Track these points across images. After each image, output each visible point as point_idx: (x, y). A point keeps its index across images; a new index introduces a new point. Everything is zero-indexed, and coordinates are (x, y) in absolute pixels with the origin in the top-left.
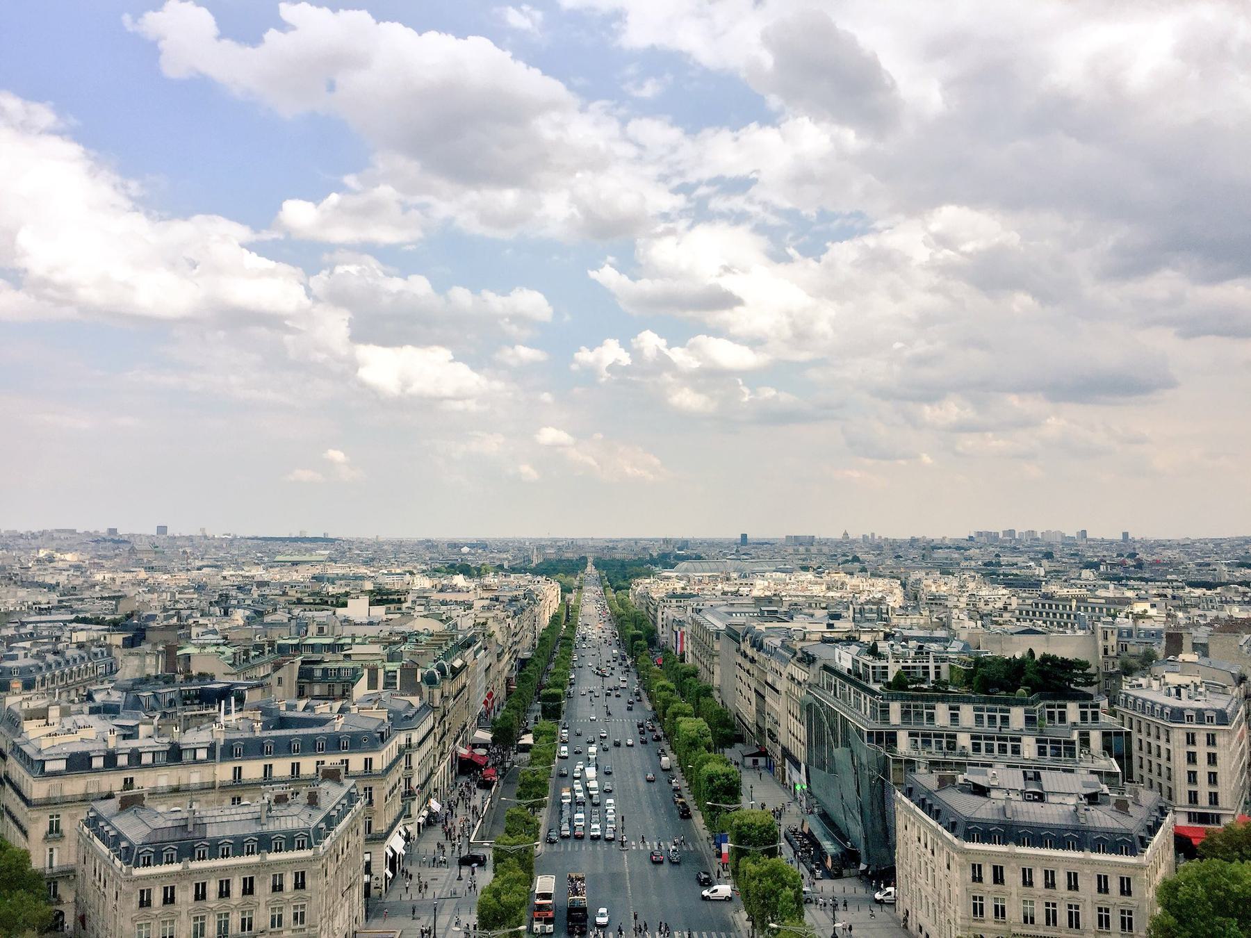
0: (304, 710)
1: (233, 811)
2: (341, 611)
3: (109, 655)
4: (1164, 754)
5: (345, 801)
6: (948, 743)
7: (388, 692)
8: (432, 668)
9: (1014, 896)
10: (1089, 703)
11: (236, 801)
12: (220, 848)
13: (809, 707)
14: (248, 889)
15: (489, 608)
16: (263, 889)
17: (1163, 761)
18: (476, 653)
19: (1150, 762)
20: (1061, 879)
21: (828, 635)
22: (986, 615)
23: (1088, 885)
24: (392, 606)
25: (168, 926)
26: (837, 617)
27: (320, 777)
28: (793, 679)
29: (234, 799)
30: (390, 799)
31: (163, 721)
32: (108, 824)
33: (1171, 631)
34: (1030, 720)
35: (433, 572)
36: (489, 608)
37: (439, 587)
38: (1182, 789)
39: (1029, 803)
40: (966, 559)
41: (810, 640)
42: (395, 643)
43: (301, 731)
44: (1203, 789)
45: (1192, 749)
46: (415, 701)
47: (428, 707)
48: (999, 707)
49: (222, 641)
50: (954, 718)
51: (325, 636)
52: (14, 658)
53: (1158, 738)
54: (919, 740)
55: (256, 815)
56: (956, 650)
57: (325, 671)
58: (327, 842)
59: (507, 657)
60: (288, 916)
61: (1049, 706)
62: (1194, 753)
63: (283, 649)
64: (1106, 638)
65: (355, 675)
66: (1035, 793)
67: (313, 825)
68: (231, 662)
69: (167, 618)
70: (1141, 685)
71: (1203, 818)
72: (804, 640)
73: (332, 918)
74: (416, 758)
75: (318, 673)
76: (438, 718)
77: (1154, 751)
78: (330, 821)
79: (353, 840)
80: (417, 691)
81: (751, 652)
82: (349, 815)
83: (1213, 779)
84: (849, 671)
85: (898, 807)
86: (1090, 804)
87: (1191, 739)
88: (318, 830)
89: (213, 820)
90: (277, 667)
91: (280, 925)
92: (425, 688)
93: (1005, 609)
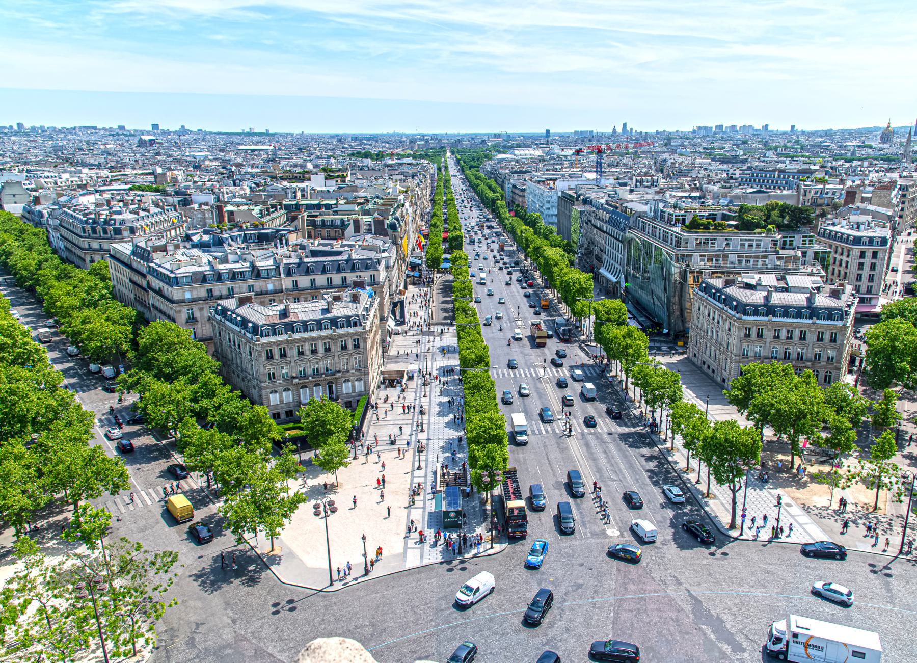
0: (319, 244)
4: (844, 264)
11: (297, 300)
16: (336, 348)
17: (842, 268)
42: (360, 204)
43: (330, 258)
45: (862, 261)
51: (306, 199)
53: (842, 254)
57: (323, 221)
58: (369, 323)
64: (805, 195)
75: (319, 223)
77: (837, 263)
78: (367, 310)
87: (862, 254)
92: (390, 231)
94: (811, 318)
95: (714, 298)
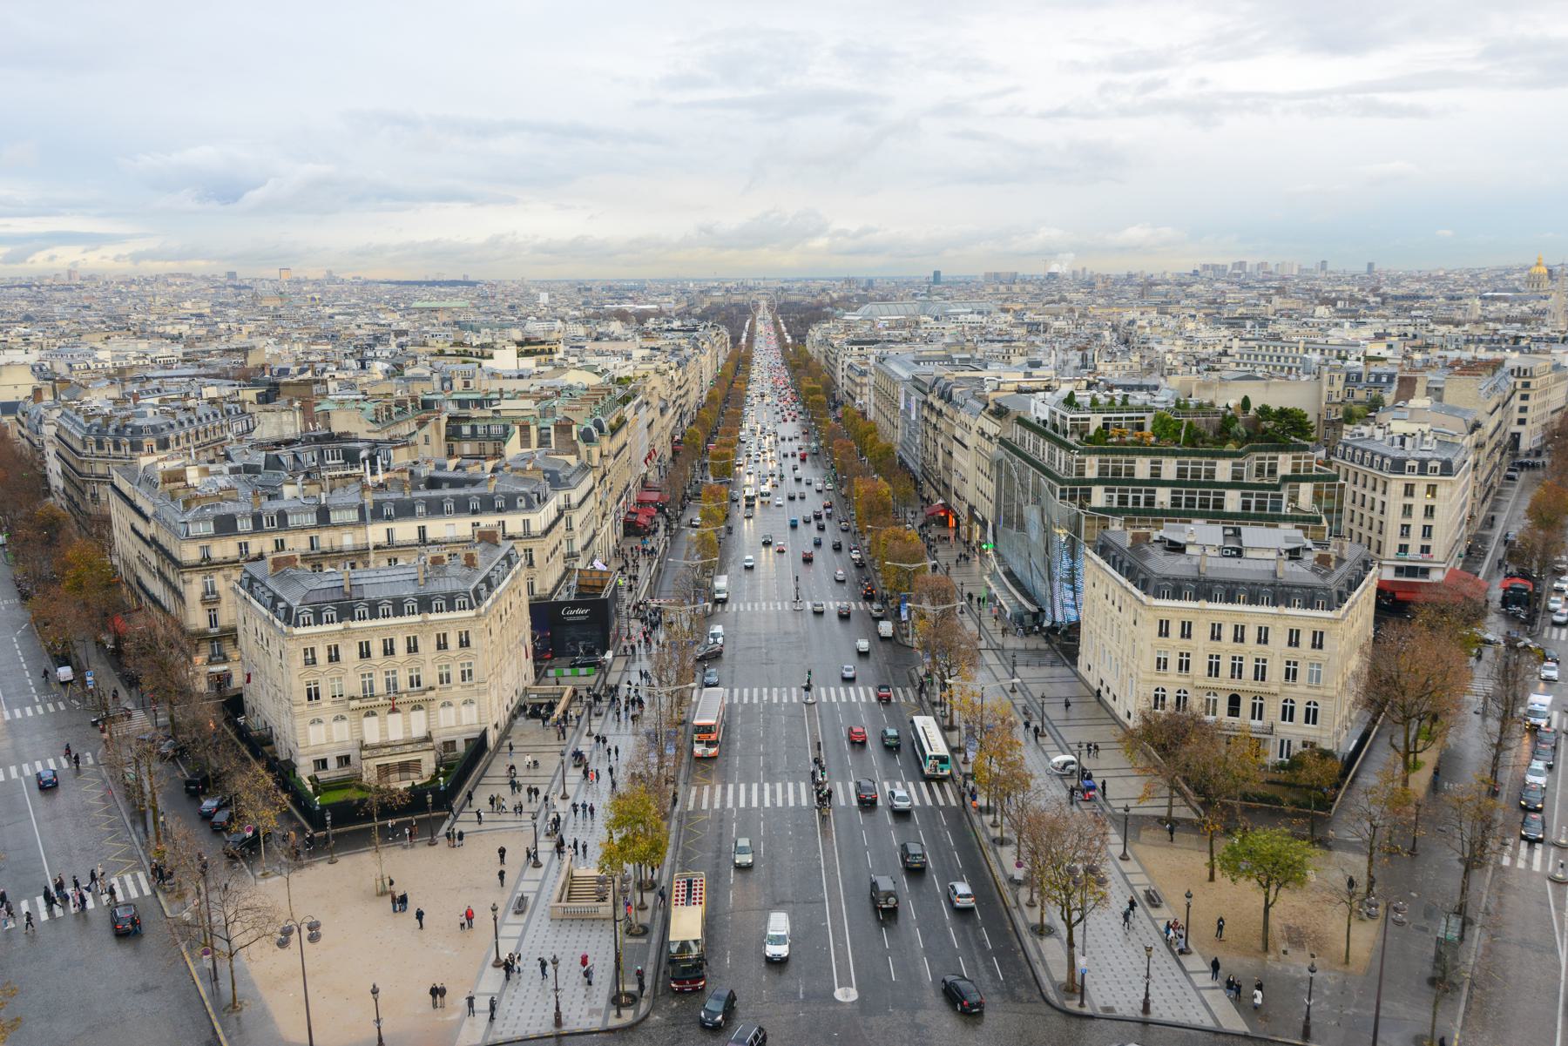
0: (457, 467)
1: (389, 573)
2: (486, 363)
3: (243, 412)
4: (1378, 507)
5: (505, 562)
6: (1146, 498)
7: (543, 450)
8: (589, 425)
9: (1201, 651)
10: (1303, 455)
11: (392, 561)
12: (380, 608)
13: (999, 464)
14: (413, 648)
15: (650, 359)
16: (427, 646)
17: (1376, 515)
18: (638, 407)
19: (1362, 515)
20: (1251, 634)
21: (1024, 385)
22: (1204, 360)
23: (1278, 639)
24: (543, 357)
25: (336, 683)
26: (1036, 364)
27: (477, 540)
28: (983, 434)
29: (390, 561)
30: (551, 560)
31: (308, 481)
32: (263, 585)
33: (1405, 375)
34: (1237, 475)
35: (586, 320)
36: (650, 359)
37: (594, 335)
38: (1392, 540)
39: (1226, 559)
40: (1187, 296)
41: (1004, 391)
42: (547, 398)
44: (1415, 541)
45: (1408, 501)
46: (572, 460)
47: (585, 468)
48: (1204, 460)
49: (361, 397)
50: (1156, 472)
52: (144, 415)
53: (1374, 489)
54: (1116, 495)
55: (412, 577)
56: (1164, 399)
58: (489, 602)
59: (671, 411)
60: (456, 675)
61: (1258, 459)
62: (1410, 506)
63: (427, 405)
64: (1331, 384)
65: (506, 434)
66: (1233, 549)
67: (472, 587)
68: (373, 418)
69: (302, 371)
70: (1362, 434)
71: (1412, 571)
72: (998, 390)
73: (500, 675)
74: (577, 518)
75: (466, 430)
76: (598, 478)
77: (1368, 505)
79: (514, 599)
80: (576, 451)
81: (938, 404)
82: (510, 576)
83: (1427, 532)
84: (1045, 422)
85: (1087, 563)
86: (1290, 559)
87: (1409, 490)
88: (477, 591)
89: (369, 581)
90: (422, 424)
91: (448, 681)
92: (582, 446)
93: (1225, 353)
94: (1275, 604)
95: (1114, 568)
